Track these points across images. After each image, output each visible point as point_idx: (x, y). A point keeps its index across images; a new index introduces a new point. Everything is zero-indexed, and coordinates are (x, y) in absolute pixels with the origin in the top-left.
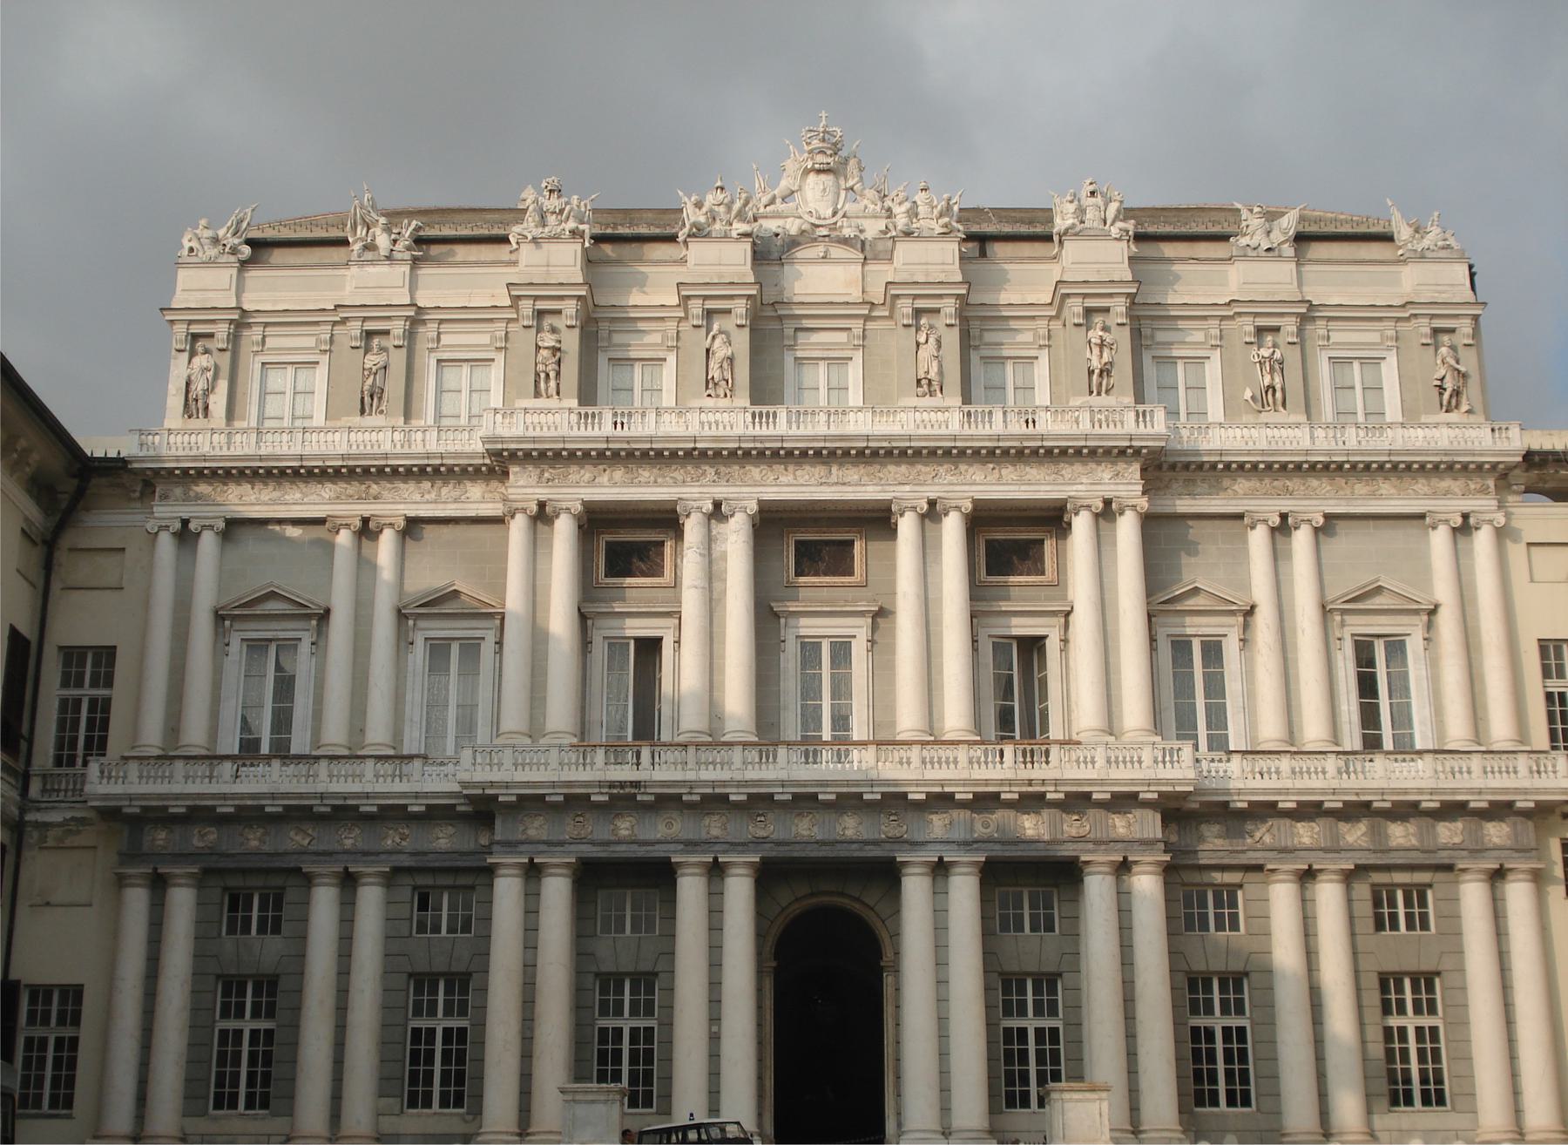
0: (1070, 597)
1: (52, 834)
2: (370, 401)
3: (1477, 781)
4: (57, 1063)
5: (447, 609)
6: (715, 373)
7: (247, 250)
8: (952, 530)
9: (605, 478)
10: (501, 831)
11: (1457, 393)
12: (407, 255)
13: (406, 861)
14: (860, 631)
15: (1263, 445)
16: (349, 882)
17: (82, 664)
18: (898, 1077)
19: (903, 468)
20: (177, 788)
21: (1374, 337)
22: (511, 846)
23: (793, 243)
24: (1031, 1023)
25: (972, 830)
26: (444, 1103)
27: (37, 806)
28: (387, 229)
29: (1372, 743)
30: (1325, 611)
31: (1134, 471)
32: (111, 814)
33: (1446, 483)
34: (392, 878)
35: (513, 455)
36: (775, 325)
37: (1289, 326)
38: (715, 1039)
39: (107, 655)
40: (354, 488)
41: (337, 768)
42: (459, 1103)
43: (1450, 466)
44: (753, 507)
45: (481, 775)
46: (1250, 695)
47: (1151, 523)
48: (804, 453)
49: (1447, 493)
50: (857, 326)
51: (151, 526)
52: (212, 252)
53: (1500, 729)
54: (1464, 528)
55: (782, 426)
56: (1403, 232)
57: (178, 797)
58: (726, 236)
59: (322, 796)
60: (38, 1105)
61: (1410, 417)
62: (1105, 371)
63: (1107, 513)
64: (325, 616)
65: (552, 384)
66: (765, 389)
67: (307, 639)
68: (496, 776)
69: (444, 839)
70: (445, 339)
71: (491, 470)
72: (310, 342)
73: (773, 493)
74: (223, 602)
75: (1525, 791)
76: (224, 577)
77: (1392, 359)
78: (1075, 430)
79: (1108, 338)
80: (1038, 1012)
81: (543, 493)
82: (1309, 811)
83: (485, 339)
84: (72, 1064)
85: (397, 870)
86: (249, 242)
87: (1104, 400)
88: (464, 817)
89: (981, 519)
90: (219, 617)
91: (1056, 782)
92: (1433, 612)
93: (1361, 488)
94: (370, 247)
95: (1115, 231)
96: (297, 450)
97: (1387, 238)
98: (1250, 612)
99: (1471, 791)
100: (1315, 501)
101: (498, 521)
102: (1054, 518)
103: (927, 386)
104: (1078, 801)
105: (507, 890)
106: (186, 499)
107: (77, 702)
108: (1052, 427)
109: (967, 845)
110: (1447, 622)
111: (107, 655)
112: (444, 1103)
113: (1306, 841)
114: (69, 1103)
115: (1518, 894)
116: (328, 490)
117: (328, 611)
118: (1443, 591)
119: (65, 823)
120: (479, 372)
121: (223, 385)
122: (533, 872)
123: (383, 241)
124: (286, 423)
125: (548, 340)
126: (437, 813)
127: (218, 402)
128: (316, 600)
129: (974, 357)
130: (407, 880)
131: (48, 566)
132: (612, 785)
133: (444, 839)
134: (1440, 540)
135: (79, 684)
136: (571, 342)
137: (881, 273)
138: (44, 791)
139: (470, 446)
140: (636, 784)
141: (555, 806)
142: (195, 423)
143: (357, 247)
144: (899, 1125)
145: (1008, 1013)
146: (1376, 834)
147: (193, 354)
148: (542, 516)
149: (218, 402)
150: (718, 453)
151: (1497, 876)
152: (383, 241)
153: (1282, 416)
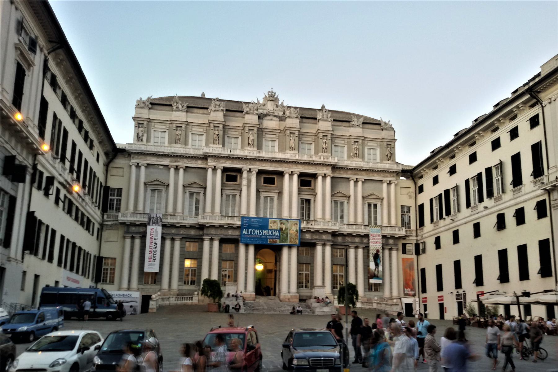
0: (316, 191)
1: (109, 226)
2: (177, 141)
3: (389, 232)
4: (110, 273)
5: (194, 186)
6: (251, 143)
7: (150, 106)
8: (295, 177)
9: (228, 162)
10: (205, 231)
11: (390, 157)
12: (185, 110)
13: (185, 236)
14: (275, 196)
15: (354, 165)
16: (173, 240)
17: (114, 191)
18: (279, 282)
19: (286, 165)
20: (138, 219)
21: (376, 145)
22: (208, 235)
23: (266, 115)
24: (304, 273)
26: (191, 284)
27: (107, 221)
28: (181, 104)
29: (370, 223)
30: (363, 198)
31: (330, 169)
32: (123, 224)
33: (386, 174)
34: (182, 239)
35: (209, 156)
36: (261, 133)
37: (360, 141)
38: (246, 273)
39: (120, 191)
40: (173, 159)
41: (173, 217)
42: (194, 284)
43: (388, 171)
44: (257, 171)
45: (202, 221)
46: (349, 213)
47: (333, 178)
48: (268, 160)
49: (387, 177)
50: (277, 134)
51: (131, 164)
52: (143, 105)
53: (393, 223)
54: (389, 184)
55: (263, 154)
56: (383, 124)
57: (138, 221)
58: (253, 114)
59: (169, 222)
60: (106, 281)
61: (382, 160)
62: (326, 148)
63: (325, 177)
64: (168, 185)
66: (259, 147)
67: (164, 190)
68: (205, 221)
69: (193, 232)
70: (193, 129)
71: (203, 158)
72: (164, 127)
73: (261, 168)
74: (147, 181)
76: (147, 175)
77: (379, 150)
78: (320, 160)
80: (306, 271)
81: (215, 164)
82: (358, 235)
83: (202, 130)
84: (114, 273)
85: (183, 238)
86: (151, 103)
87: (325, 154)
88: (197, 228)
89: (301, 175)
90: (145, 184)
91: (313, 228)
92: (382, 199)
93: (371, 174)
94: (177, 108)
95: (329, 120)
96: (163, 151)
97: (379, 124)
98: (349, 197)
100: (362, 177)
101: (205, 168)
102: (314, 176)
103: (292, 148)
104: (317, 232)
105: (206, 243)
106: (138, 159)
107: (114, 200)
108: (315, 159)
110: (385, 201)
111: (120, 191)
112: (191, 284)
113: (357, 241)
114: (113, 282)
115: (394, 253)
118: (385, 195)
119: (112, 225)
120: (201, 137)
121: (145, 135)
122: (212, 240)
123: (180, 106)
124: (159, 144)
126: (192, 227)
127: (145, 138)
128: (166, 182)
129: (300, 142)
130: (184, 240)
131: (107, 171)
132: (229, 224)
133: (193, 232)
134: (385, 185)
135: (114, 196)
136: (221, 133)
137: (283, 124)
139: (200, 153)
140: (233, 224)
141: (217, 228)
142: (140, 143)
143: (175, 108)
145: (300, 271)
147: (139, 127)
148: (215, 169)
149: (145, 138)
150: (251, 159)
151: (391, 249)
152: (180, 106)
153: (357, 159)
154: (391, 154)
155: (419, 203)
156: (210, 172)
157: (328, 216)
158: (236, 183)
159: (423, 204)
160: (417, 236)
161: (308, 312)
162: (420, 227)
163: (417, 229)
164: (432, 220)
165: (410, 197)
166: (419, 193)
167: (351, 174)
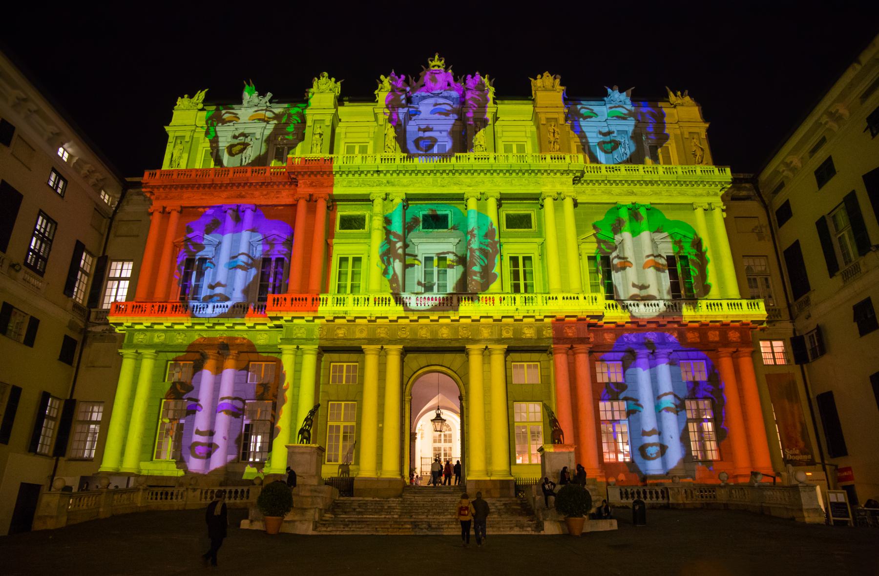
22: (288, 340)
25: (501, 335)
33: (700, 189)
47: (576, 204)
49: (701, 195)
54: (708, 210)
65: (319, 148)
75: (747, 316)
79: (556, 130)
81: (311, 190)
99: (723, 316)
106: (166, 198)
109: (500, 341)
116: (225, 194)
117: (220, 243)
121: (185, 156)
125: (319, 131)
134: (699, 212)
138: (96, 318)
144: (468, 470)
146: (681, 335)
154: (702, 149)
155: (786, 244)
156: (302, 206)
157: (575, 284)
158: (361, 230)
159: (798, 241)
160: (792, 318)
161: (522, 527)
162: (796, 297)
163: (789, 306)
164: (833, 268)
165: (761, 238)
166: (780, 226)
167: (620, 195)
